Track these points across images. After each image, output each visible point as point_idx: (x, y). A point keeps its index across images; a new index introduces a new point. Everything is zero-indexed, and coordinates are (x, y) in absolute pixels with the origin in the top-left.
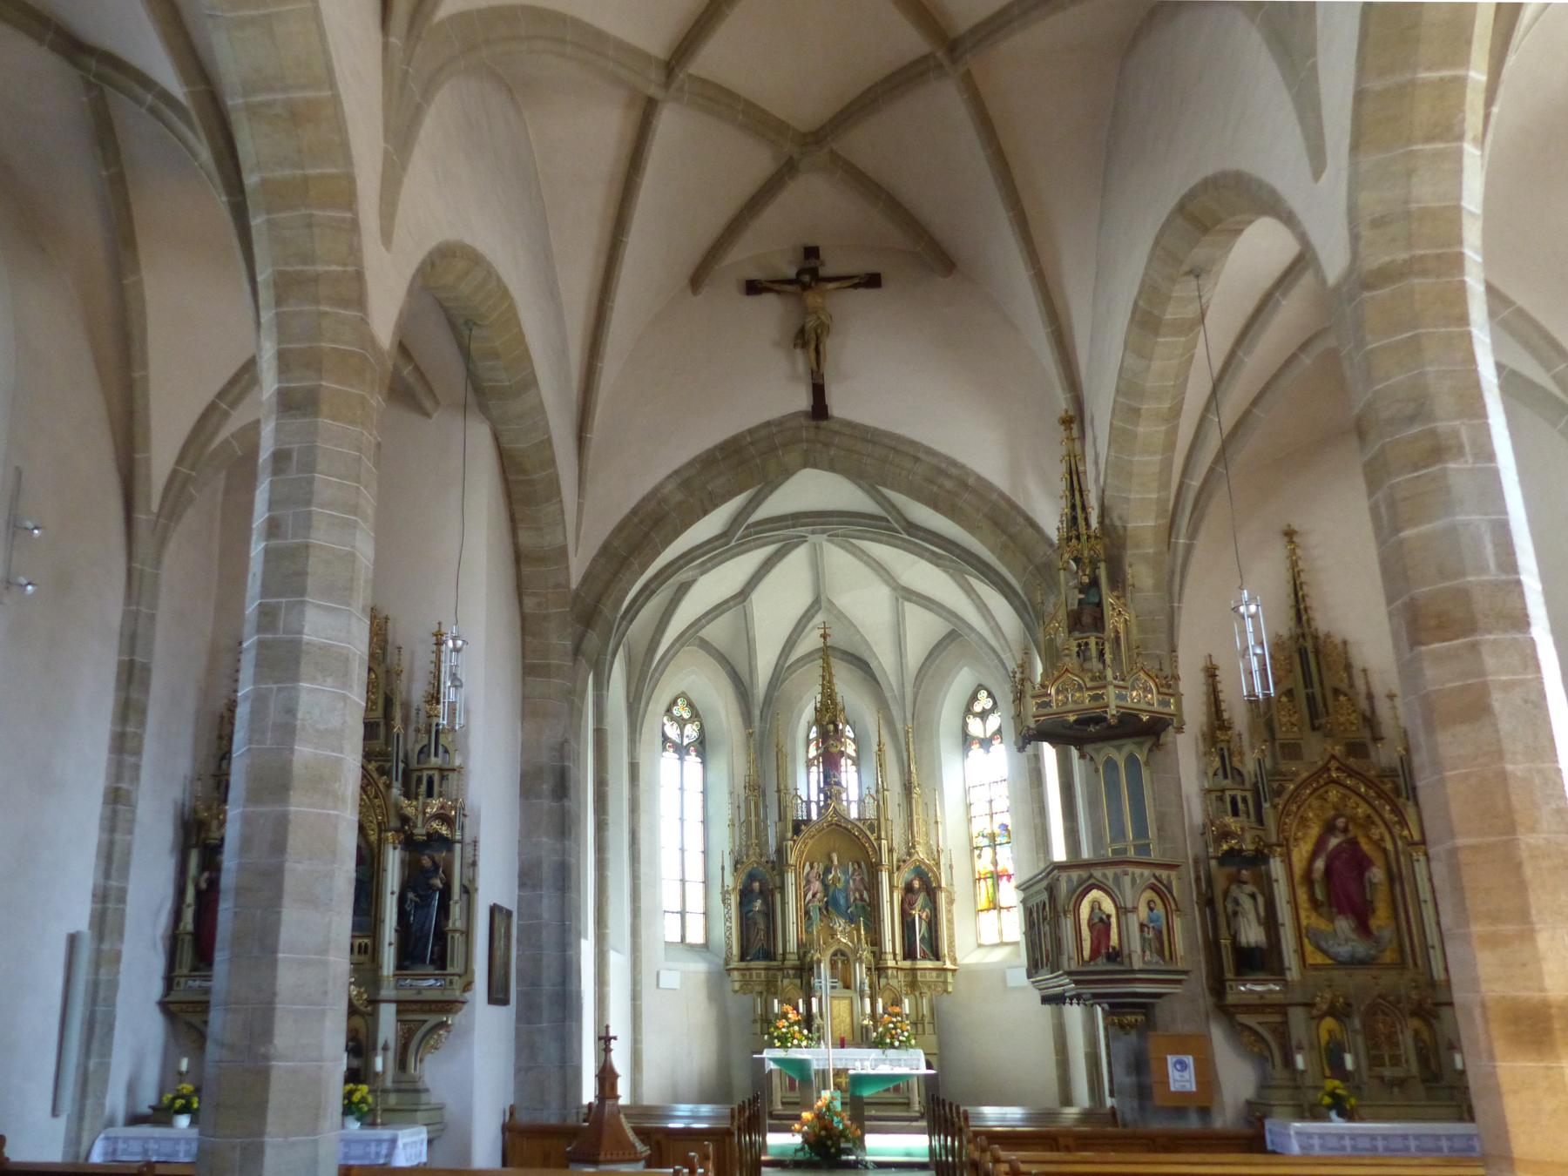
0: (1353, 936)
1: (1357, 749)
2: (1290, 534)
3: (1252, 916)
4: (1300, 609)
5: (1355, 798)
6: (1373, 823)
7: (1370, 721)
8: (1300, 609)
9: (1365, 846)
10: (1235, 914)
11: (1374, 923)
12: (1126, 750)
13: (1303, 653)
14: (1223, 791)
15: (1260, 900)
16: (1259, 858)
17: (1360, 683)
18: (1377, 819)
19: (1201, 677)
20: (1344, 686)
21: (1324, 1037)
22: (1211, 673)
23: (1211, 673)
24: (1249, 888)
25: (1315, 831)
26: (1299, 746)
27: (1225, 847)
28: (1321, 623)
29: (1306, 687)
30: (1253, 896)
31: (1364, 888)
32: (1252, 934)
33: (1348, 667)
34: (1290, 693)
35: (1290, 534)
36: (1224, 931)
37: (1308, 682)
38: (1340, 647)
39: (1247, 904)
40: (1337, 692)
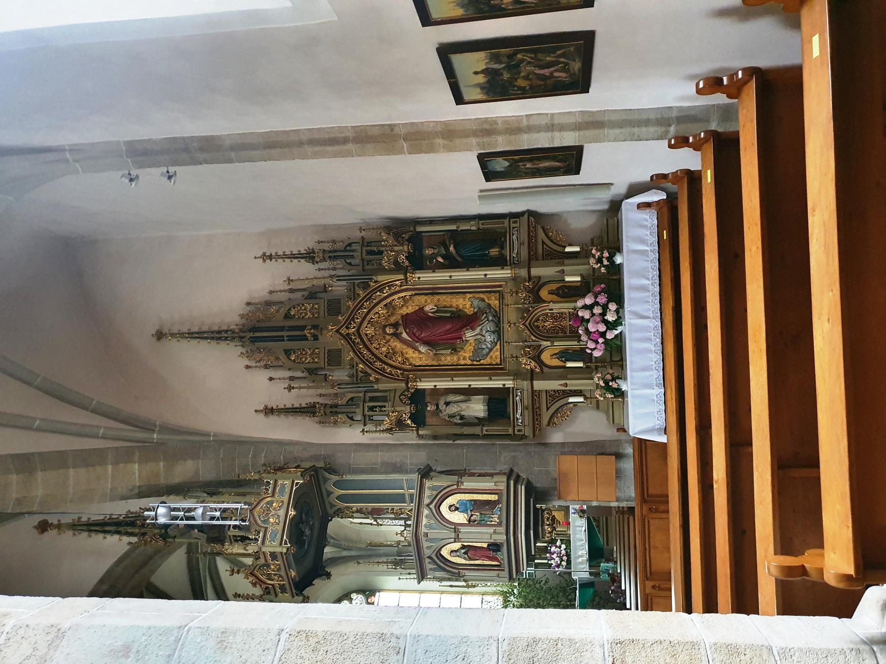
0: (478, 330)
1: (334, 307)
2: (160, 335)
3: (463, 406)
4: (218, 335)
5: (371, 315)
6: (390, 303)
7: (312, 295)
8: (218, 335)
9: (409, 309)
10: (462, 417)
11: (469, 311)
12: (332, 488)
13: (254, 340)
15: (451, 398)
16: (418, 398)
17: (283, 297)
18: (388, 300)
19: (273, 419)
20: (283, 311)
21: (556, 362)
22: (269, 411)
23: (269, 411)
24: (442, 406)
25: (397, 345)
26: (329, 351)
27: (409, 422)
29: (283, 340)
30: (447, 404)
31: (441, 317)
32: (477, 408)
33: (268, 304)
34: (287, 352)
35: (160, 335)
36: (477, 430)
37: (281, 339)
38: (248, 308)
39: (453, 409)
40: (287, 316)
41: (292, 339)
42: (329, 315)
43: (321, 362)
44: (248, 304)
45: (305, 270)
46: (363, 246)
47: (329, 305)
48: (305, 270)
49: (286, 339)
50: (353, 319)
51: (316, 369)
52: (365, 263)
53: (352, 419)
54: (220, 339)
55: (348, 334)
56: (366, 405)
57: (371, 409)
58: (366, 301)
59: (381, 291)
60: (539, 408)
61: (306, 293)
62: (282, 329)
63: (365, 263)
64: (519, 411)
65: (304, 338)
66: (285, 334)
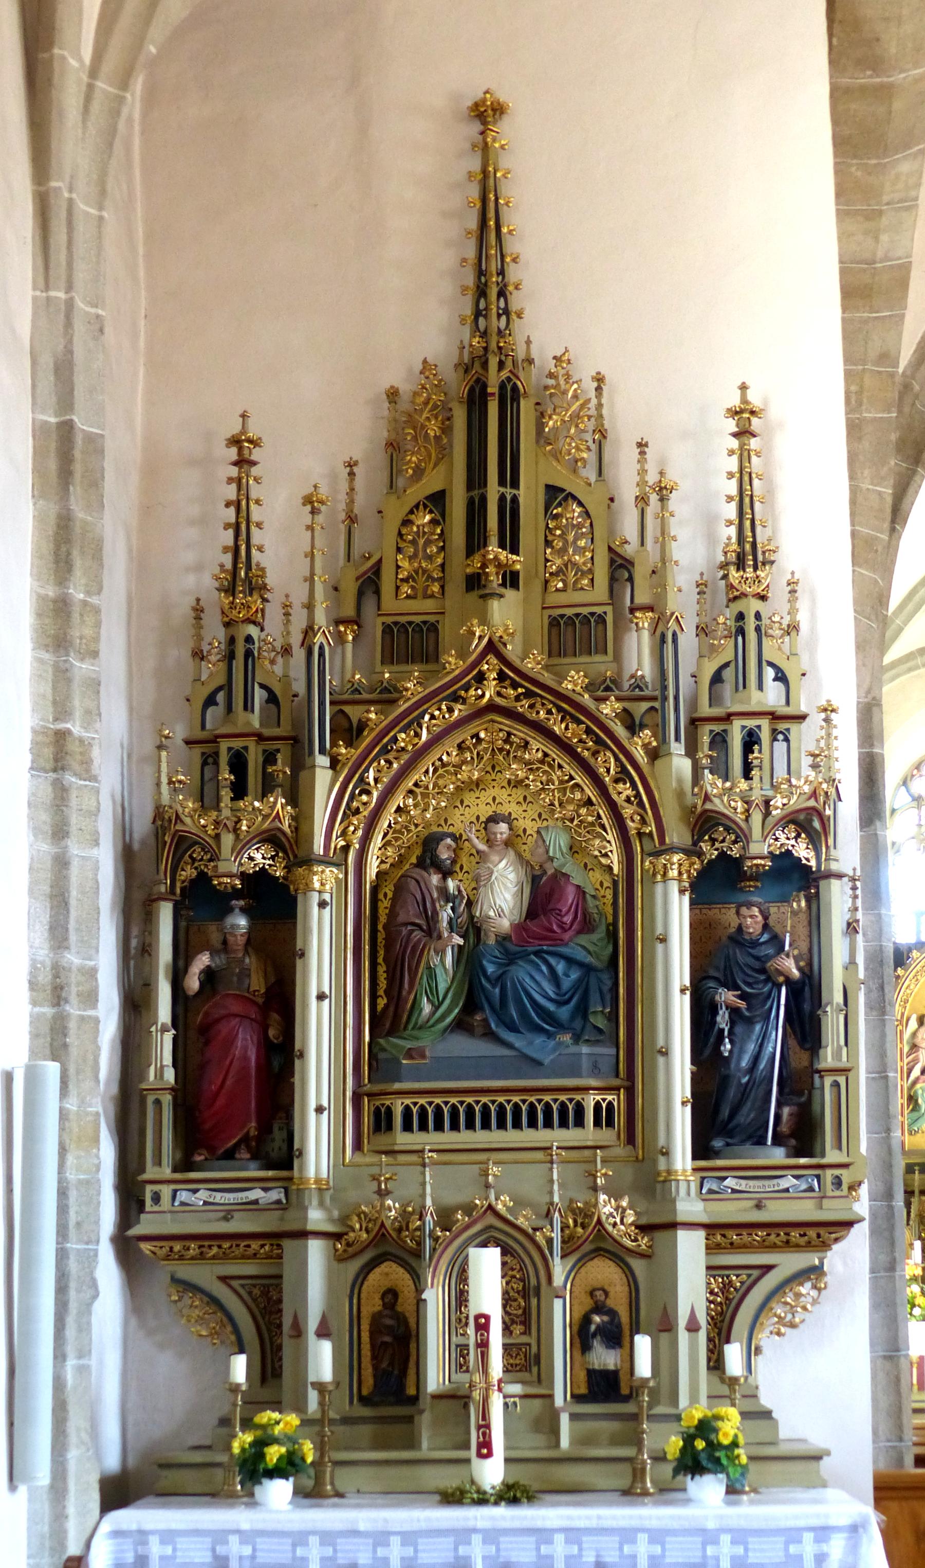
4: (488, 286)
13: (476, 399)
14: (215, 740)
28: (545, 327)
34: (437, 501)
37: (476, 477)
41: (476, 511)
42: (554, 623)
43: (398, 603)
44: (599, 379)
45: (693, 548)
46: (774, 717)
47: (586, 620)
48: (693, 548)
49: (476, 493)
50: (529, 694)
51: (377, 592)
52: (717, 728)
53: (210, 701)
54: (481, 292)
55: (481, 678)
56: (251, 743)
57: (238, 763)
58: (588, 731)
59: (623, 776)
60: (224, 1257)
61: (630, 550)
62: (510, 475)
63: (717, 728)
64: (219, 1197)
65: (475, 540)
66: (493, 491)
